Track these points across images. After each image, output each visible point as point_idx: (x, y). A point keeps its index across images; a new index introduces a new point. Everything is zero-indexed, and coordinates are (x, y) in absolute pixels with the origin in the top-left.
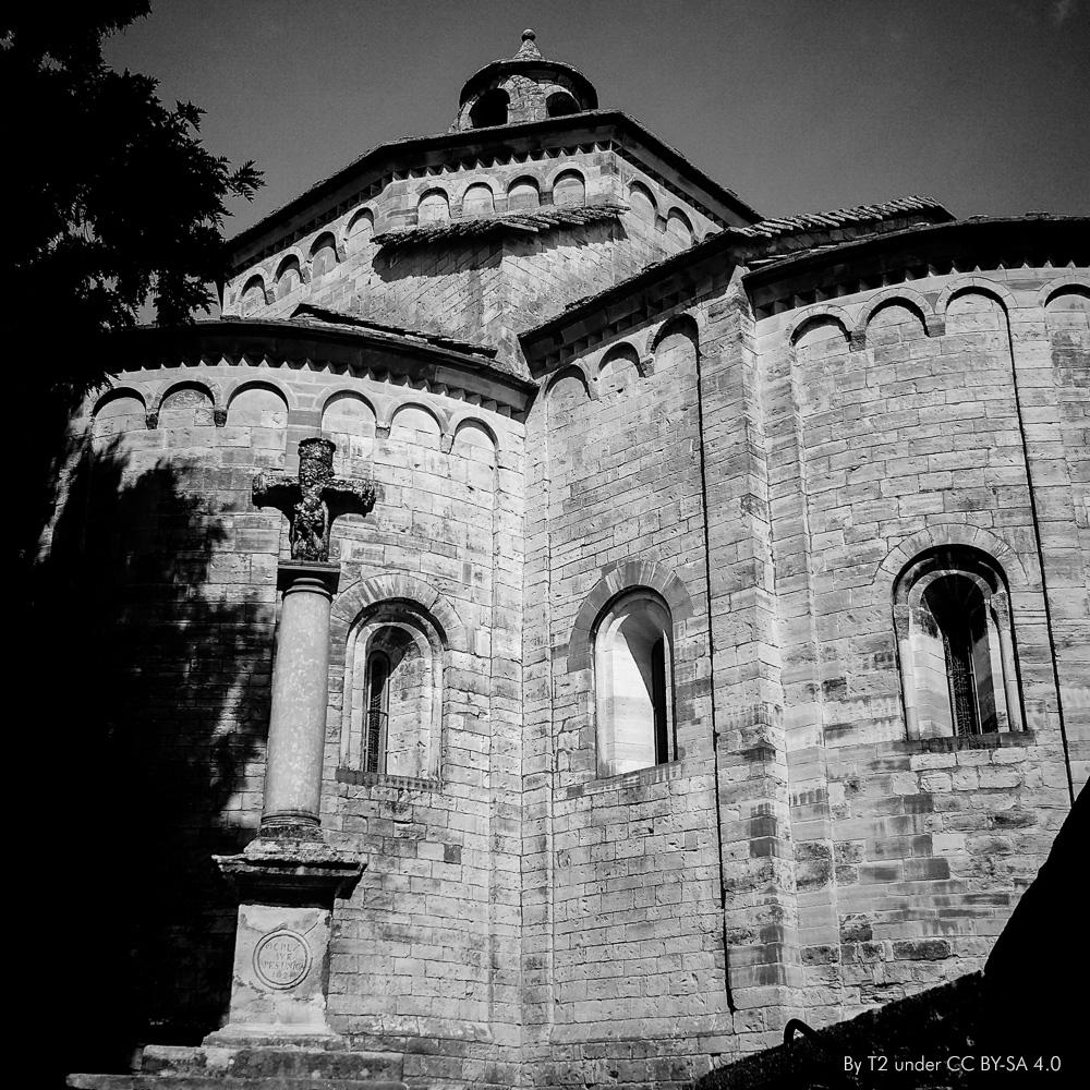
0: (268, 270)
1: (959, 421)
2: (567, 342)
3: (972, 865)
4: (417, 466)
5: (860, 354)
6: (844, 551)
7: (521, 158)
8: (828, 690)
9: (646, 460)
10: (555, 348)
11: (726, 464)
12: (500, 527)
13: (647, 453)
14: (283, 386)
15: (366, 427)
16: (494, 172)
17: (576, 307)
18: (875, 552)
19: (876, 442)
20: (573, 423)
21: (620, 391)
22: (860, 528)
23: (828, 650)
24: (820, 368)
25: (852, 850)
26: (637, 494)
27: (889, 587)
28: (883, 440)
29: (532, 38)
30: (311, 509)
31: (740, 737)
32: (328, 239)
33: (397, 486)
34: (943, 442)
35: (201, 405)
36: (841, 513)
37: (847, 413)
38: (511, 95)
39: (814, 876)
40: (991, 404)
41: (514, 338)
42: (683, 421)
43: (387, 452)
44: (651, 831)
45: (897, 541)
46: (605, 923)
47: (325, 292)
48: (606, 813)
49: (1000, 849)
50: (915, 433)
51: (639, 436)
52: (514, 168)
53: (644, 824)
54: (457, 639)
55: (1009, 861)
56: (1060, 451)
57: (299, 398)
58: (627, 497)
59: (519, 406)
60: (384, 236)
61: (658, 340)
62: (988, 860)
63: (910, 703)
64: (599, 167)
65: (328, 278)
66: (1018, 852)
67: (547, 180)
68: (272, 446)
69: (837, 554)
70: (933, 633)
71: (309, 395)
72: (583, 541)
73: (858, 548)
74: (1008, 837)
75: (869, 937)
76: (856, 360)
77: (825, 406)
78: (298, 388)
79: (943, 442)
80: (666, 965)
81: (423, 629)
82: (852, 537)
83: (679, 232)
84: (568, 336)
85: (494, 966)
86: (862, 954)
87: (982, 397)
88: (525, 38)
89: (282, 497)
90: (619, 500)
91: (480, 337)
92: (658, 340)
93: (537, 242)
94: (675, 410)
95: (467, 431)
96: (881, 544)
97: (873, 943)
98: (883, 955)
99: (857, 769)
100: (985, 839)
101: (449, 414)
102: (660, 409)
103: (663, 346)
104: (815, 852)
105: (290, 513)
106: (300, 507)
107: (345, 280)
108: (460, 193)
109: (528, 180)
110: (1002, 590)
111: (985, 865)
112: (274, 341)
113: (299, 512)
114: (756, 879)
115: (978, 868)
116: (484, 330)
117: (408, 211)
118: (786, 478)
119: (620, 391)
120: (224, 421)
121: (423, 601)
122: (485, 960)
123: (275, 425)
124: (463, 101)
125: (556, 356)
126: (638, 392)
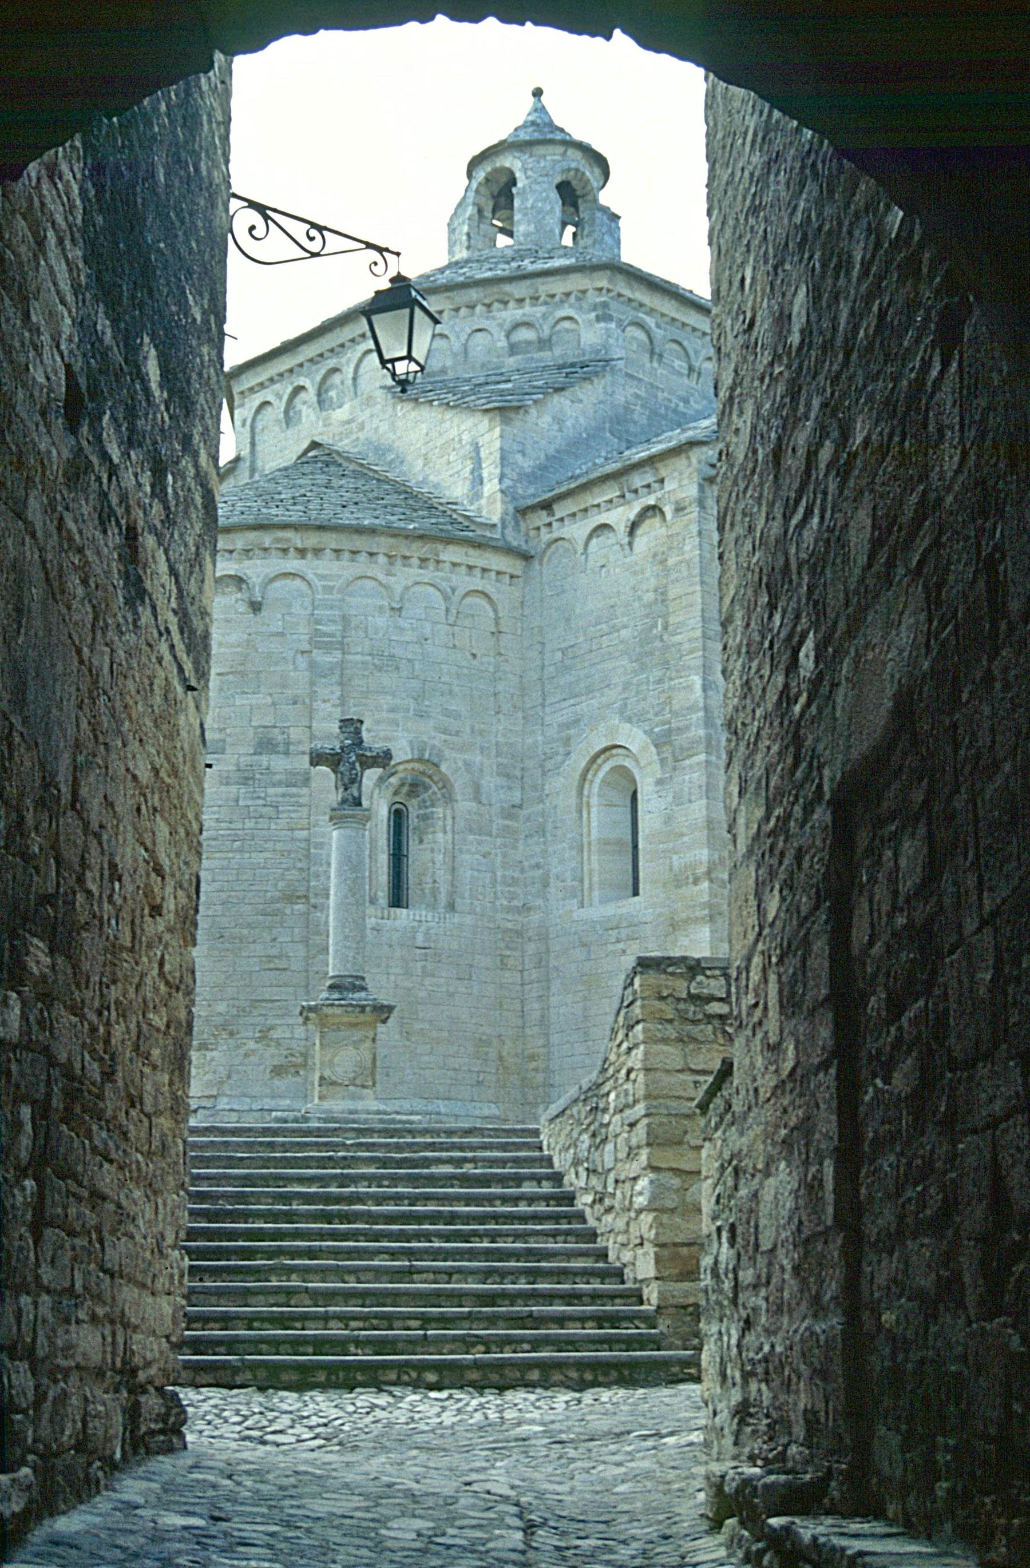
0: (279, 397)
2: (558, 516)
7: (521, 301)
12: (500, 687)
13: (625, 627)
14: (310, 576)
15: (381, 607)
16: (494, 318)
20: (564, 592)
32: (335, 370)
33: (409, 660)
35: (239, 596)
38: (518, 175)
41: (511, 508)
43: (402, 629)
44: (624, 951)
47: (336, 429)
51: (619, 611)
52: (513, 313)
57: (324, 587)
58: (608, 665)
59: (519, 573)
61: (633, 527)
64: (593, 315)
65: (340, 414)
67: (545, 327)
68: (301, 630)
71: (331, 584)
72: (572, 701)
78: (322, 577)
83: (677, 363)
85: (501, 1058)
89: (333, 760)
92: (633, 527)
95: (469, 600)
101: (453, 590)
102: (634, 589)
103: (639, 532)
107: (352, 420)
108: (463, 337)
109: (528, 325)
112: (299, 535)
116: (483, 502)
120: (260, 609)
122: (493, 1054)
123: (303, 612)
124: (470, 175)
125: (550, 524)
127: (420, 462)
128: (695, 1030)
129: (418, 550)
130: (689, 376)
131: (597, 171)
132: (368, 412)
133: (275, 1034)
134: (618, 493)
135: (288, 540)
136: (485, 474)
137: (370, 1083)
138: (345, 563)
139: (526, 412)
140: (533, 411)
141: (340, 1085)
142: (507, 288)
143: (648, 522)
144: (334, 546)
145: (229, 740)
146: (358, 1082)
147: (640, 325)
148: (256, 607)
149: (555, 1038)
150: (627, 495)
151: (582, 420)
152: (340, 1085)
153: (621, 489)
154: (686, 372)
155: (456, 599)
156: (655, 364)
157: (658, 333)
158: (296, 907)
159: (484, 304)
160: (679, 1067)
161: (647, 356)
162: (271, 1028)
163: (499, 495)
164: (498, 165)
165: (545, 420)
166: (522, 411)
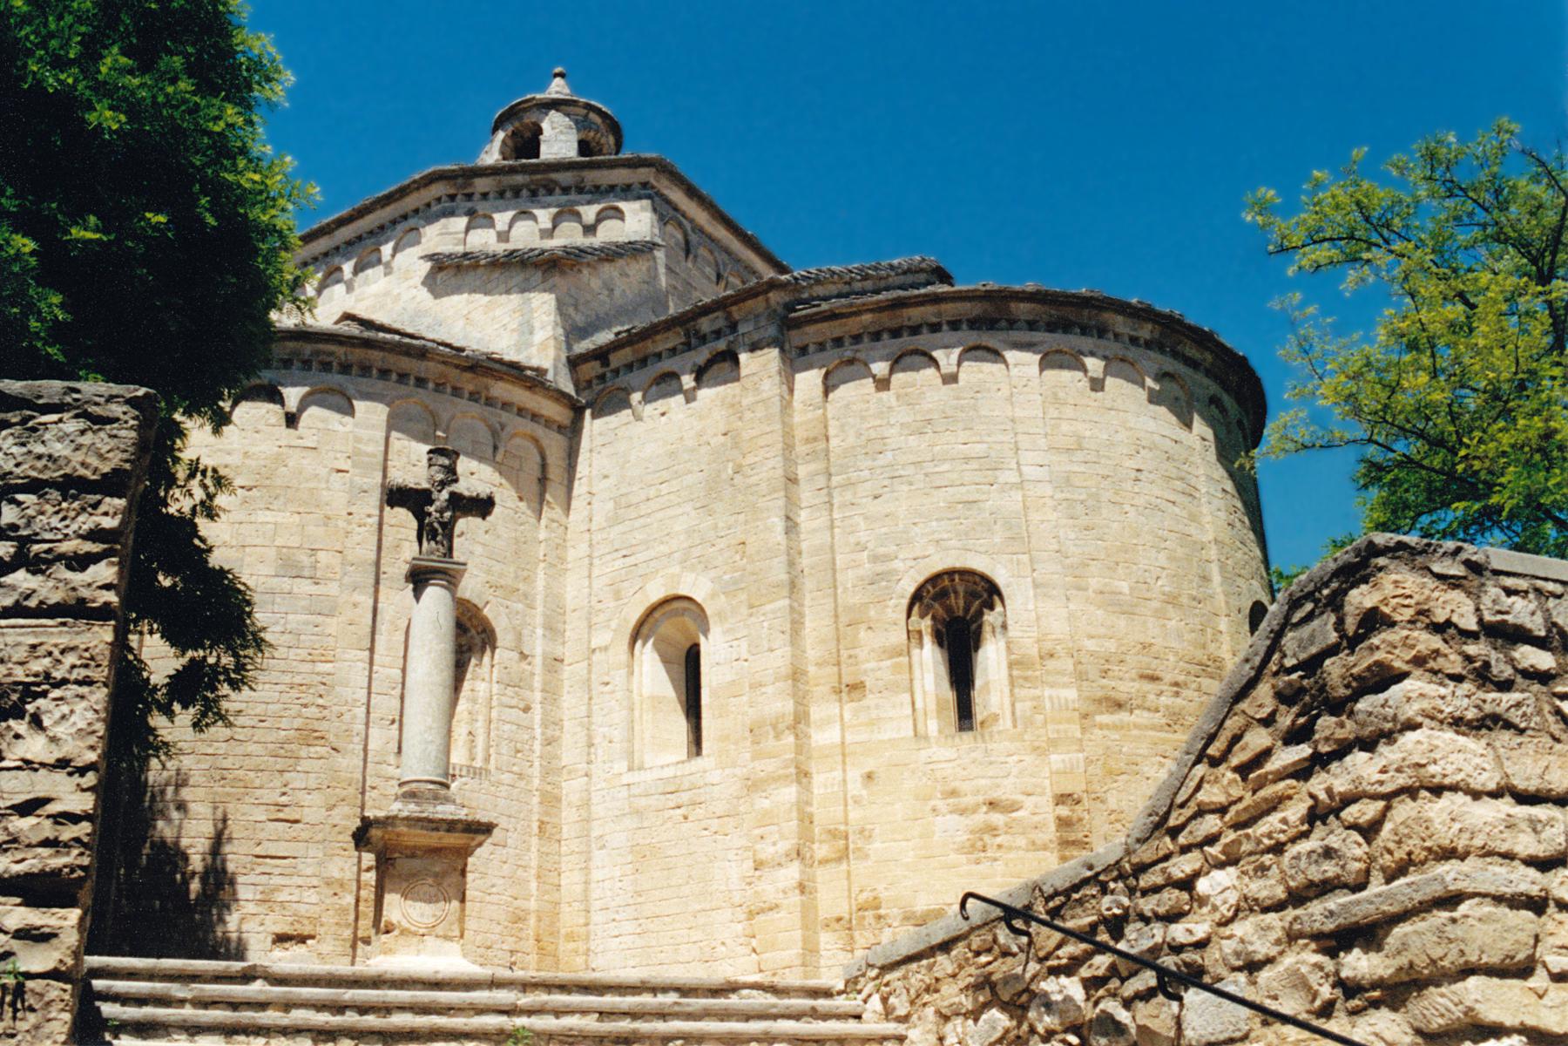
1: (967, 459)
3: (967, 844)
4: (472, 474)
5: (884, 395)
6: (867, 568)
8: (849, 692)
9: (689, 479)
10: (601, 371)
11: (764, 485)
17: (624, 335)
18: (896, 571)
19: (897, 474)
21: (663, 414)
22: (882, 550)
23: (850, 657)
24: (847, 406)
25: (867, 833)
26: (680, 511)
27: (905, 602)
28: (902, 473)
29: (561, 75)
30: (441, 511)
31: (772, 734)
34: (955, 476)
36: (863, 536)
37: (874, 447)
39: (833, 856)
40: (993, 446)
41: (564, 359)
42: (723, 445)
45: (912, 563)
46: (640, 900)
48: (643, 802)
49: (992, 830)
50: (930, 468)
53: (678, 811)
54: (503, 637)
55: (999, 840)
56: (1048, 490)
60: (434, 255)
62: (981, 840)
63: (919, 704)
66: (1006, 833)
68: (338, 447)
69: (861, 572)
70: (940, 644)
73: (880, 568)
74: (997, 818)
75: (878, 908)
76: (881, 399)
77: (851, 440)
79: (955, 476)
80: (697, 935)
81: (475, 627)
82: (875, 559)
84: (616, 360)
86: (872, 921)
87: (987, 439)
88: (556, 75)
90: (660, 515)
91: (529, 358)
93: (585, 272)
94: (715, 435)
96: (898, 564)
97: (882, 912)
98: (889, 921)
99: (870, 764)
100: (981, 817)
101: (503, 427)
104: (834, 836)
105: (420, 515)
106: (431, 509)
110: (999, 608)
111: (979, 844)
113: (430, 514)
114: (783, 860)
115: (973, 846)
117: (456, 233)
118: (817, 501)
119: (663, 414)
121: (476, 601)
123: (340, 428)
126: (681, 416)
127: (461, 323)
128: (1503, 701)
129: (468, 383)
130: (718, 283)
131: (611, 140)
132: (406, 284)
133: (282, 896)
134: (683, 340)
135: (331, 354)
136: (537, 324)
137: (457, 933)
138: (391, 384)
139: (580, 271)
140: (585, 272)
141: (415, 934)
142: (554, 176)
143: (715, 367)
144: (379, 364)
145: (247, 559)
146: (440, 930)
147: (680, 225)
148: (291, 420)
149: (597, 917)
150: (693, 341)
151: (628, 292)
152: (415, 934)
153: (687, 334)
154: (714, 278)
155: (504, 435)
156: (690, 265)
157: (693, 238)
158: (312, 749)
159: (529, 190)
160: (1492, 786)
161: (682, 254)
162: (277, 889)
163: (552, 342)
164: (526, 121)
165: (595, 283)
166: (575, 269)
